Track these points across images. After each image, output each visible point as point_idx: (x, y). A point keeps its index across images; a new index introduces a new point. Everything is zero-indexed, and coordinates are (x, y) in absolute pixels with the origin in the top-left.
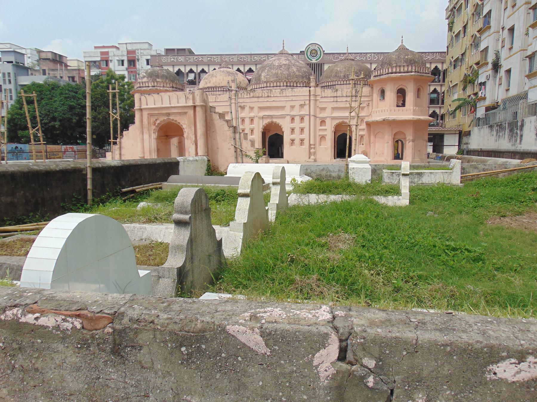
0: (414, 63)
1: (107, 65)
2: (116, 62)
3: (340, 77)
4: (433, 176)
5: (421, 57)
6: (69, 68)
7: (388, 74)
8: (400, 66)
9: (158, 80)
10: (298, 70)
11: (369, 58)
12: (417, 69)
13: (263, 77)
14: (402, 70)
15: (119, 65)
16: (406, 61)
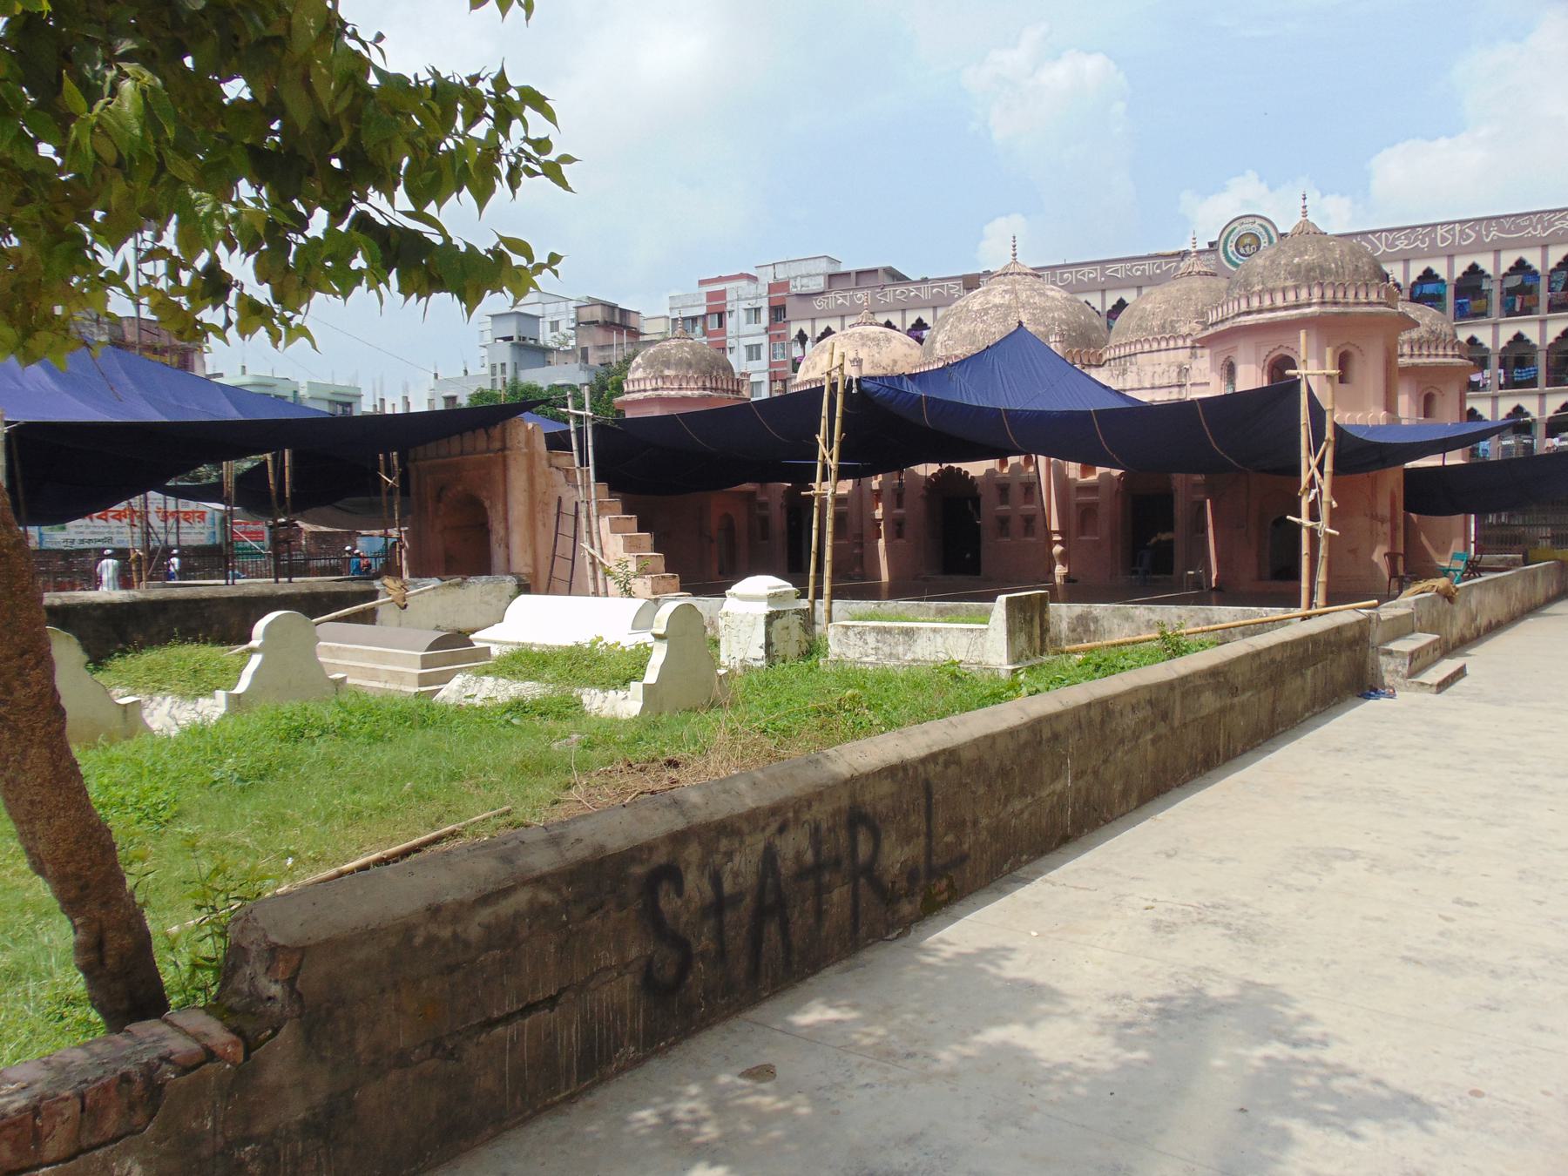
0: (1322, 275)
1: (721, 324)
2: (743, 315)
3: (1150, 330)
4: (939, 640)
5: (1353, 251)
6: (646, 338)
7: (1239, 315)
8: (1272, 292)
9: (667, 372)
10: (1035, 320)
11: (1444, 239)
12: (1329, 294)
13: (938, 345)
14: (1279, 302)
15: (748, 322)
16: (1295, 273)
